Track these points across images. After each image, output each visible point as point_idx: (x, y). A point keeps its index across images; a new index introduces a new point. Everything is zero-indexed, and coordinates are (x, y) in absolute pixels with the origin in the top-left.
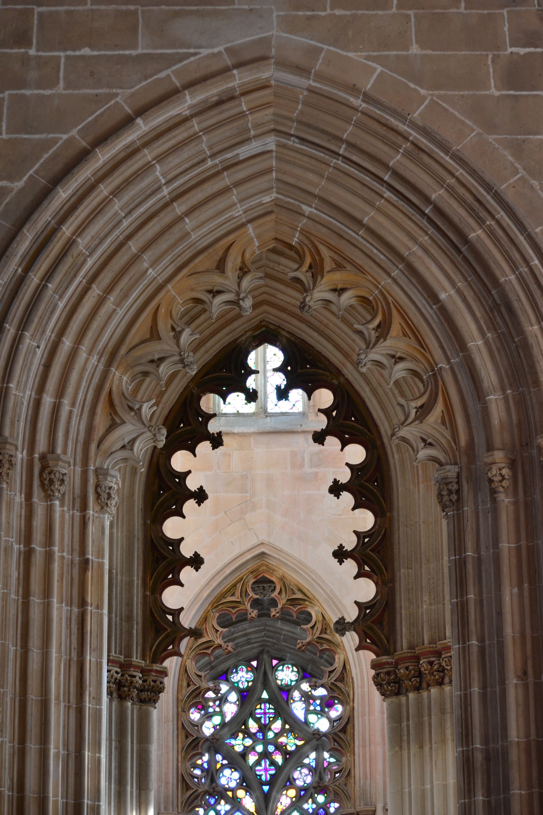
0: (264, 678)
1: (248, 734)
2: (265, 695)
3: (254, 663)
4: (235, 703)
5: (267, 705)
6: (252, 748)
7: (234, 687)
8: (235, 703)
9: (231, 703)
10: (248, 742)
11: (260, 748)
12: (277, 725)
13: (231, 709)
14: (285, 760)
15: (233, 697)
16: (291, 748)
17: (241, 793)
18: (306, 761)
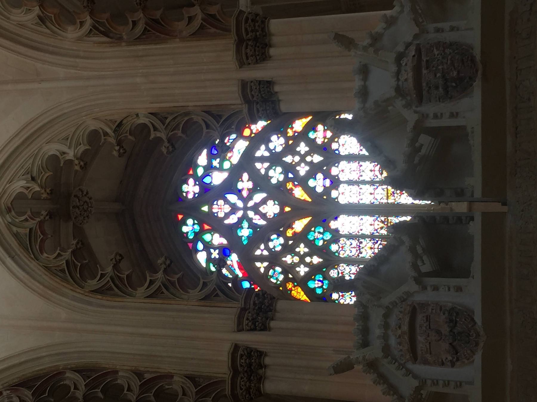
0: (192, 208)
1: (238, 225)
2: (205, 209)
3: (180, 217)
4: (212, 235)
5: (215, 206)
6: (250, 220)
7: (198, 236)
8: (212, 235)
9: (212, 239)
10: (245, 224)
11: (251, 214)
12: (232, 198)
13: (218, 240)
14: (261, 191)
15: (207, 237)
16: (250, 185)
17: (289, 233)
18: (263, 172)
